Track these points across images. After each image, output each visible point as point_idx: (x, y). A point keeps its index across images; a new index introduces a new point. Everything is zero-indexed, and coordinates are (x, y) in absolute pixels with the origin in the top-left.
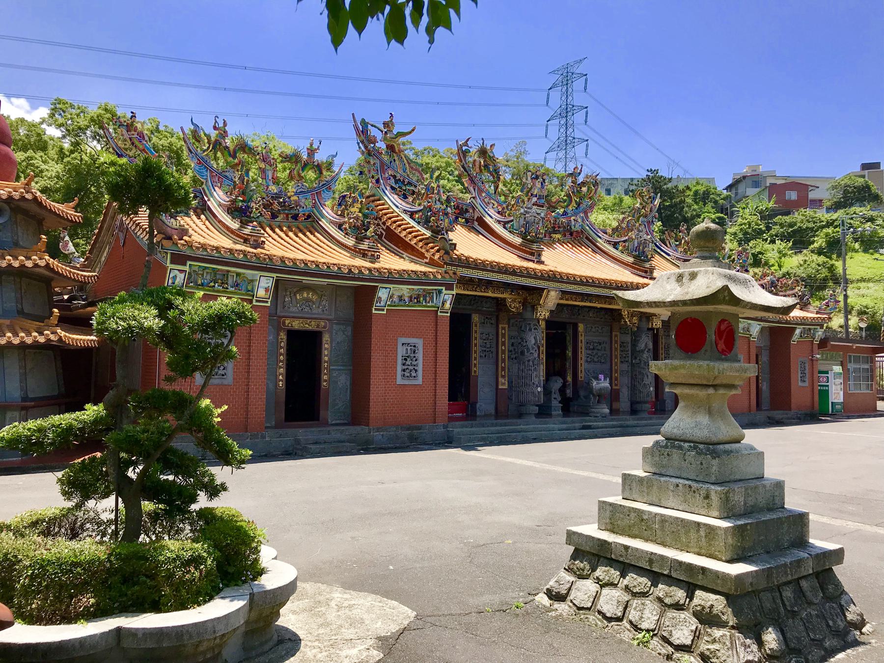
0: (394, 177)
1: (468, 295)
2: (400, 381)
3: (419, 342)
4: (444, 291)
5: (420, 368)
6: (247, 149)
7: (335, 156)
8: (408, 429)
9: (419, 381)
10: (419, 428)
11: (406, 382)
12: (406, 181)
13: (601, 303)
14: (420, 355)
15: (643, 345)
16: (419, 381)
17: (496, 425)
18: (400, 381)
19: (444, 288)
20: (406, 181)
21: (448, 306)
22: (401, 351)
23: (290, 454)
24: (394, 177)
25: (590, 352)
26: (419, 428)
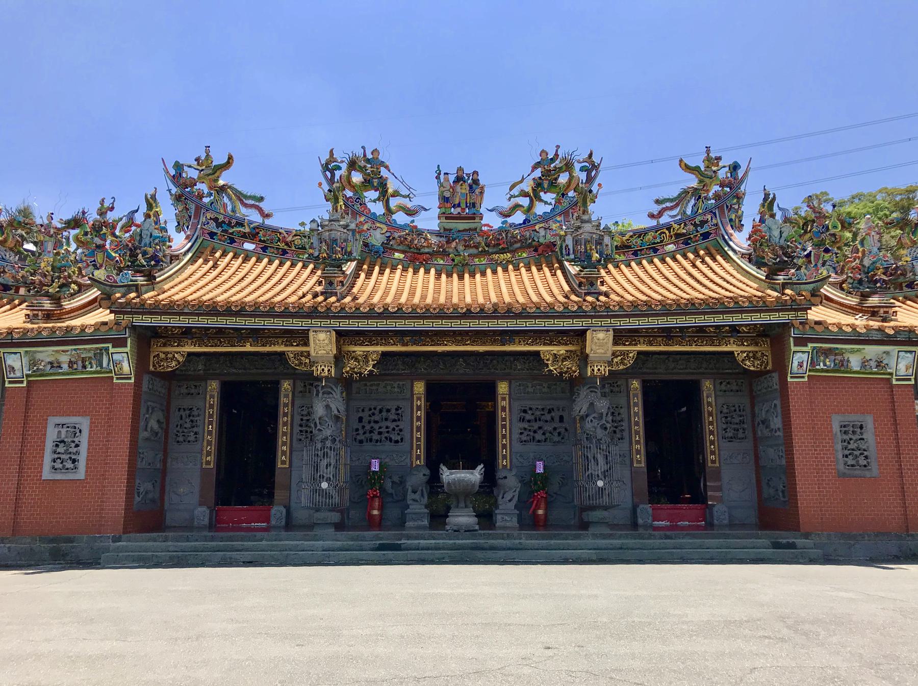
0: (216, 220)
1: (204, 354)
2: (47, 474)
3: (84, 423)
4: (111, 350)
5: (48, 457)
6: (15, 224)
7: (426, 210)
8: (51, 541)
9: (81, 474)
10: (70, 540)
11: (59, 477)
12: (234, 221)
13: (484, 344)
14: (84, 439)
15: (585, 408)
16: (81, 474)
17: (212, 539)
18: (47, 474)
19: (110, 345)
20: (234, 221)
21: (126, 368)
22: (52, 435)
23: (81, 564)
24: (216, 220)
25: (526, 425)
26: (70, 540)
